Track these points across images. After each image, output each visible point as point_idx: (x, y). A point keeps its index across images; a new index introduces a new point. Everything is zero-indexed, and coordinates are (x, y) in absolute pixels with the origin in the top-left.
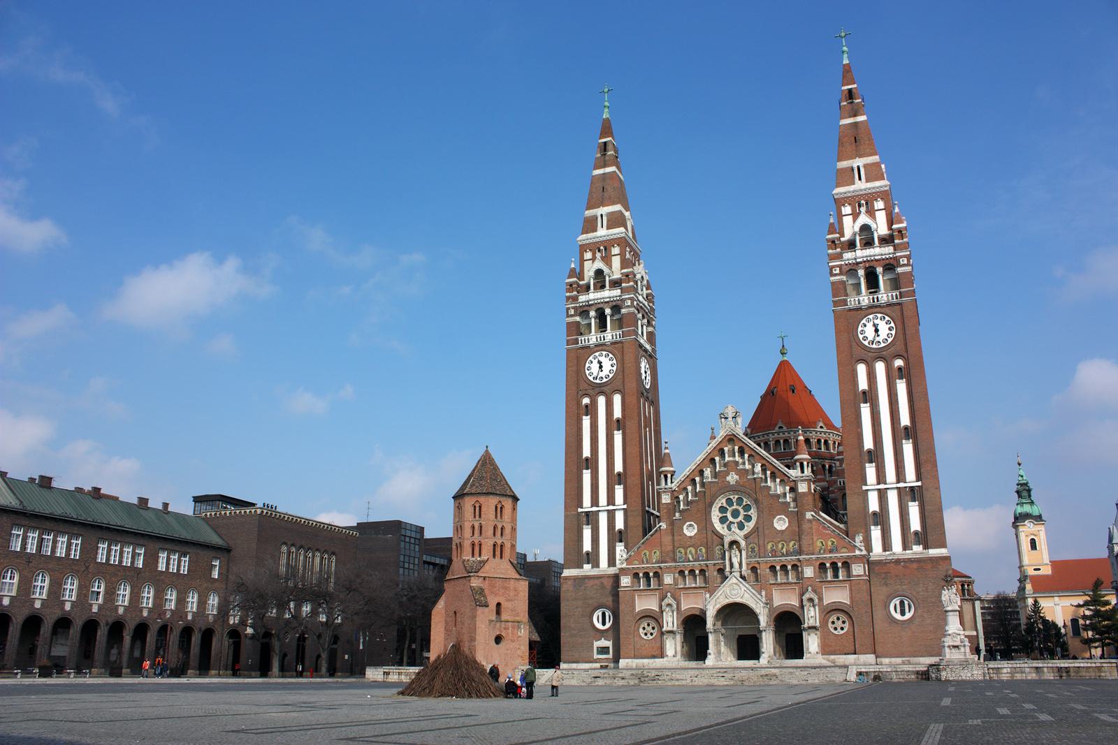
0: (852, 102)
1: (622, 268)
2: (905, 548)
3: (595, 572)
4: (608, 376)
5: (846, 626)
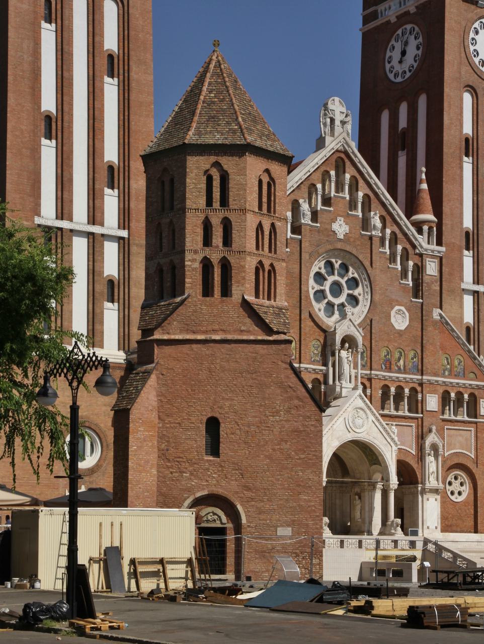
5: (466, 490)
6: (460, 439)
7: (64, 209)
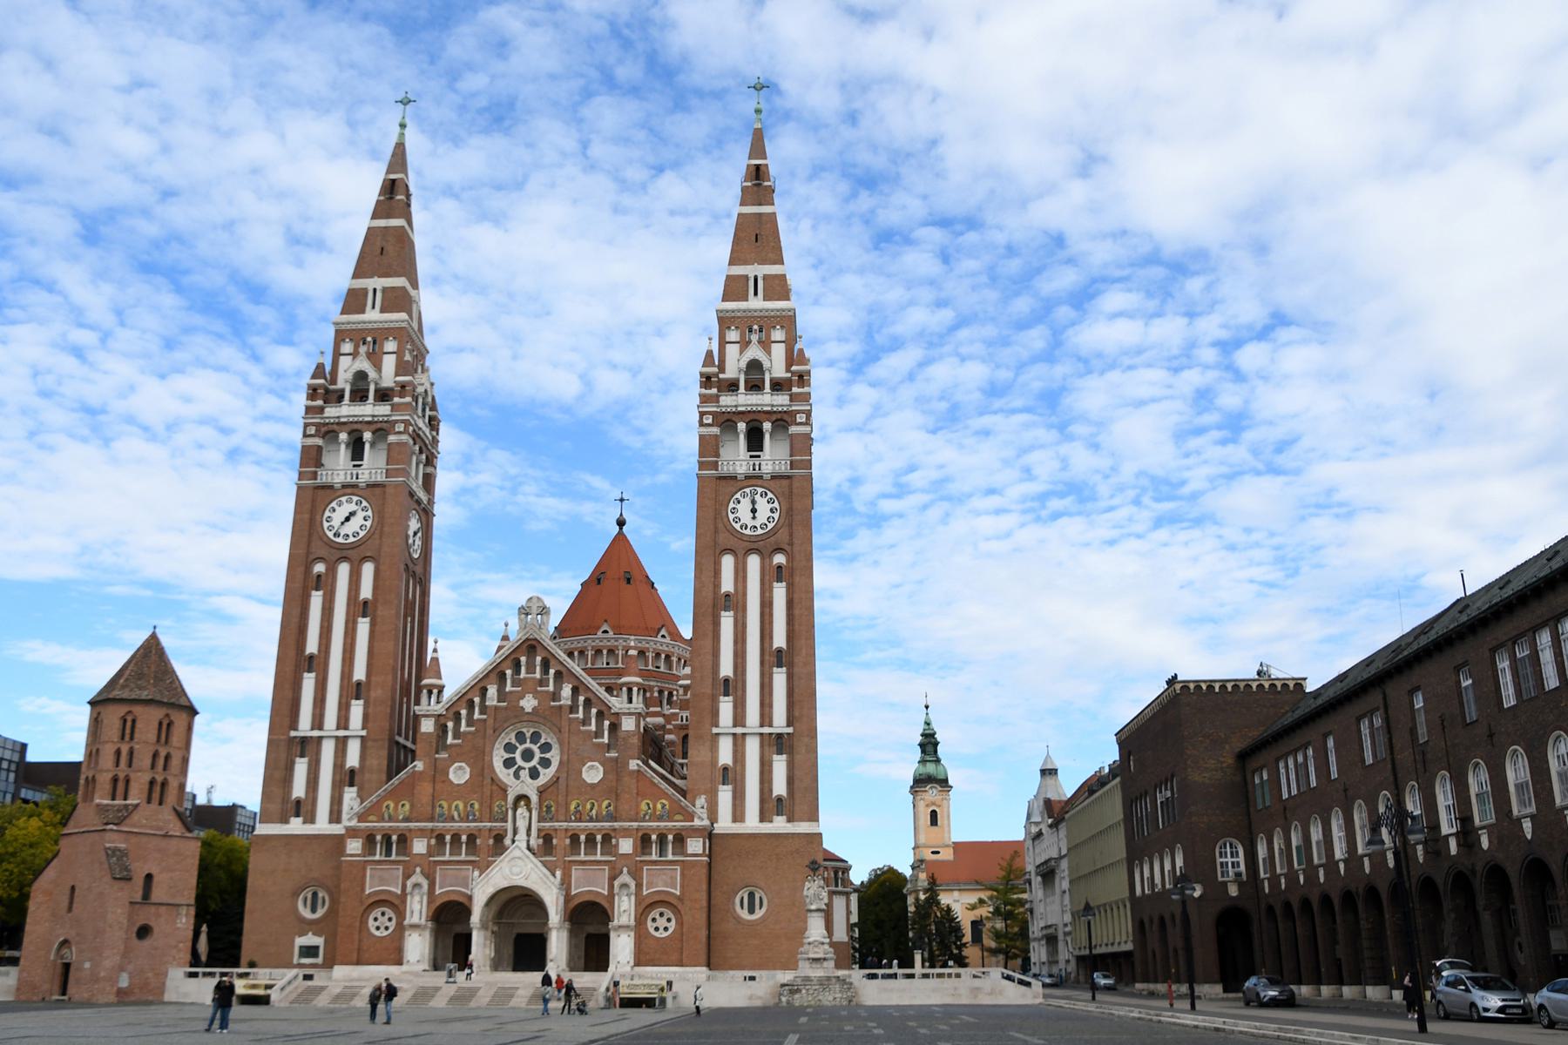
0: (759, 185)
1: (397, 375)
2: (762, 820)
3: (309, 829)
4: (358, 533)
5: (672, 925)
6: (664, 877)
7: (318, 723)
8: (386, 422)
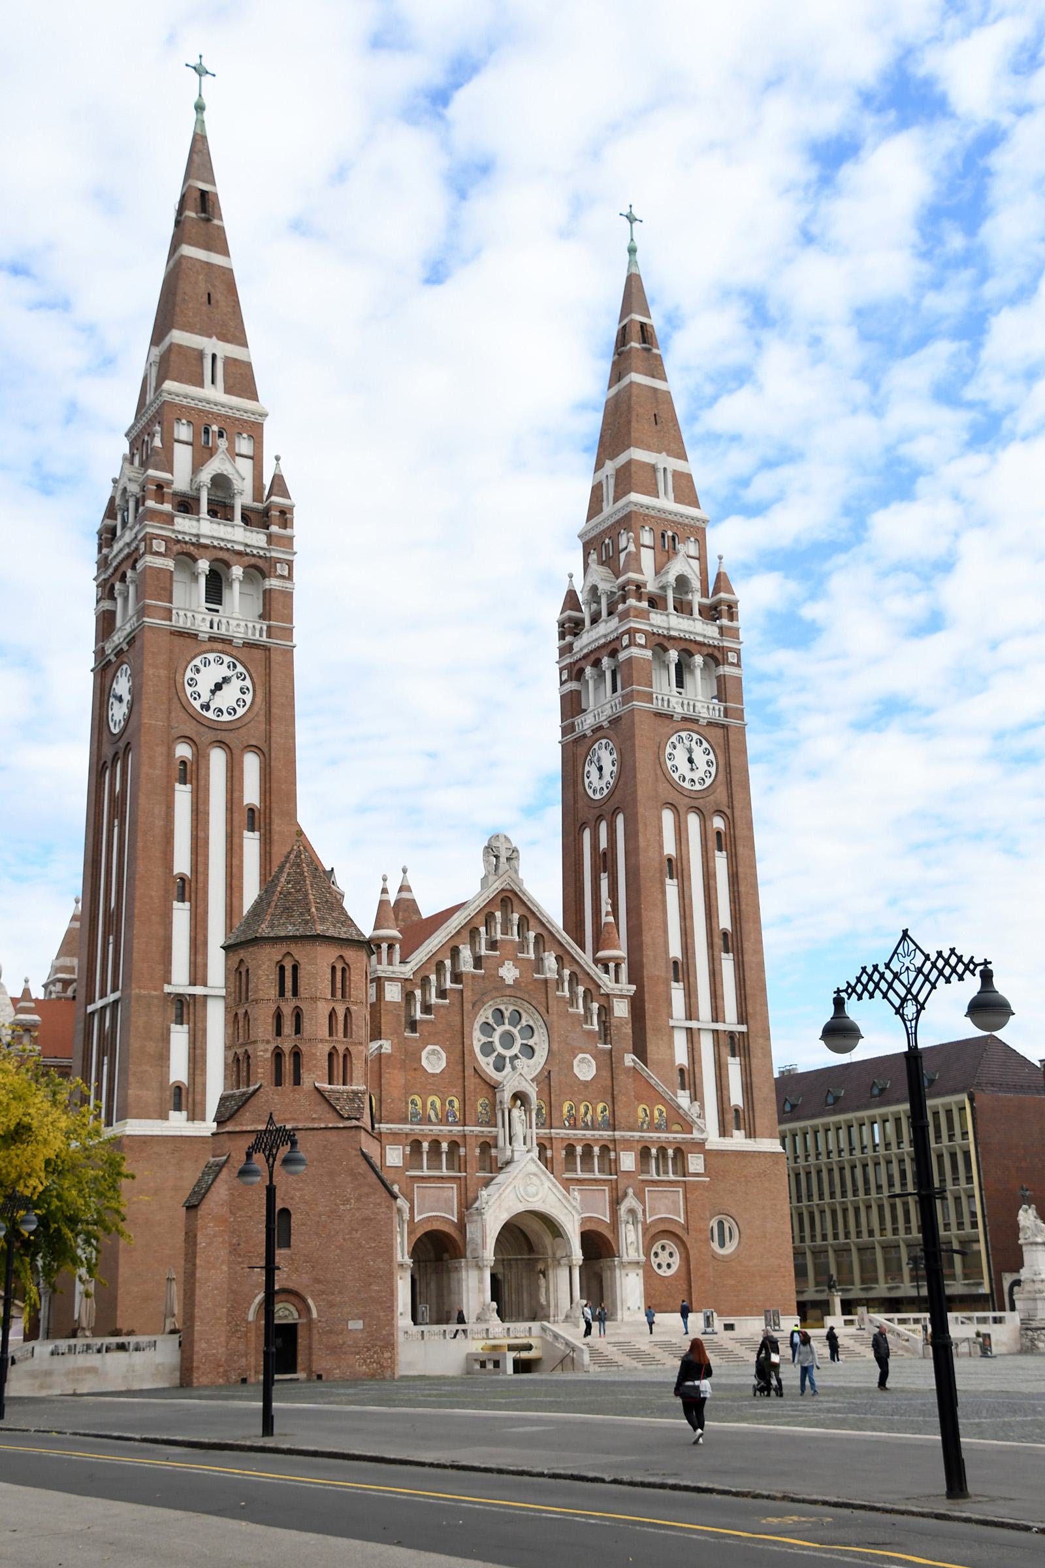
4: (234, 710)
5: (676, 1261)
7: (198, 975)
8: (260, 557)
